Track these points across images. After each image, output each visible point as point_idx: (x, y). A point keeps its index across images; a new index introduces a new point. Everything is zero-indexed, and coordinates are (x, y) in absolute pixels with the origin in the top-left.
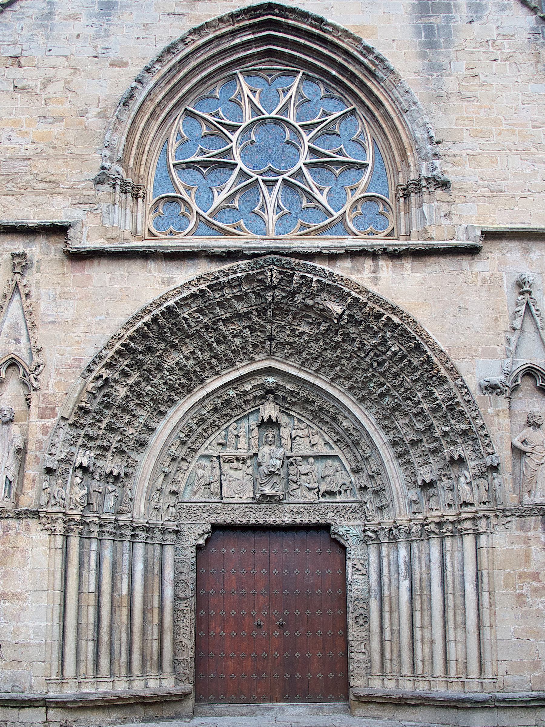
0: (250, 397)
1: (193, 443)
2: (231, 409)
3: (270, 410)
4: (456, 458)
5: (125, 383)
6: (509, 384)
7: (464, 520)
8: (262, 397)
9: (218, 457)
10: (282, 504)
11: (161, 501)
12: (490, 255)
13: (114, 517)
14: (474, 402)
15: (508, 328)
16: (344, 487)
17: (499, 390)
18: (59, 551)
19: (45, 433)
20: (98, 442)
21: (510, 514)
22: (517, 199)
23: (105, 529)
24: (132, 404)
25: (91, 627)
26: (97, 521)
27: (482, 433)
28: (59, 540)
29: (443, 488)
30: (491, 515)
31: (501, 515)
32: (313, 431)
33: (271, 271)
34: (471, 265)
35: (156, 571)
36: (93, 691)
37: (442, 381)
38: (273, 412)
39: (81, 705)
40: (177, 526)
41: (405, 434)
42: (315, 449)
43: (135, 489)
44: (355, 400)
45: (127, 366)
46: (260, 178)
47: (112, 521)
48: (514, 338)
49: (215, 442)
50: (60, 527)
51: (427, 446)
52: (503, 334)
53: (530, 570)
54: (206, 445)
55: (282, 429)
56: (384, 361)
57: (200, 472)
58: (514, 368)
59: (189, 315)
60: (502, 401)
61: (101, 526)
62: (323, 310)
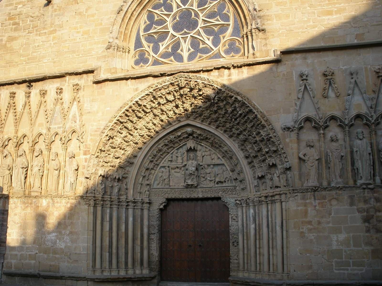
0: (181, 138)
1: (156, 161)
2: (173, 144)
3: (191, 144)
4: (271, 164)
5: (120, 137)
6: (297, 126)
7: (275, 195)
8: (187, 137)
9: (169, 167)
10: (197, 188)
11: (142, 189)
12: (287, 62)
13: (117, 197)
14: (278, 137)
15: (296, 98)
16: (227, 179)
17: (291, 130)
18: (92, 213)
19: (86, 161)
20: (109, 164)
21: (296, 192)
22: (300, 33)
23: (114, 203)
24: (124, 145)
25: (108, 247)
26: (109, 199)
27: (283, 151)
28: (92, 208)
29: (268, 179)
30: (288, 192)
31: (292, 192)
32: (212, 152)
33: (181, 80)
34: (277, 68)
35: (139, 221)
36: (109, 274)
37: (264, 127)
38: (192, 145)
39: (101, 280)
40: (149, 200)
41: (251, 153)
42: (214, 161)
43: (129, 184)
44: (228, 137)
45: (120, 129)
46: (180, 36)
47: (117, 199)
48: (298, 103)
49: (167, 160)
50: (92, 203)
51: (260, 158)
52: (294, 101)
53: (307, 220)
54: (163, 161)
55: (198, 152)
56: (237, 118)
57: (160, 174)
58: (300, 118)
59: (147, 103)
60: (293, 135)
61: (112, 201)
62: (207, 96)
